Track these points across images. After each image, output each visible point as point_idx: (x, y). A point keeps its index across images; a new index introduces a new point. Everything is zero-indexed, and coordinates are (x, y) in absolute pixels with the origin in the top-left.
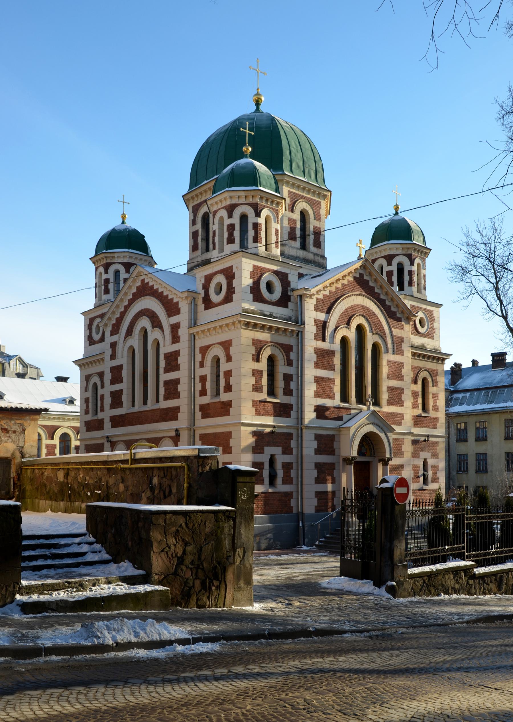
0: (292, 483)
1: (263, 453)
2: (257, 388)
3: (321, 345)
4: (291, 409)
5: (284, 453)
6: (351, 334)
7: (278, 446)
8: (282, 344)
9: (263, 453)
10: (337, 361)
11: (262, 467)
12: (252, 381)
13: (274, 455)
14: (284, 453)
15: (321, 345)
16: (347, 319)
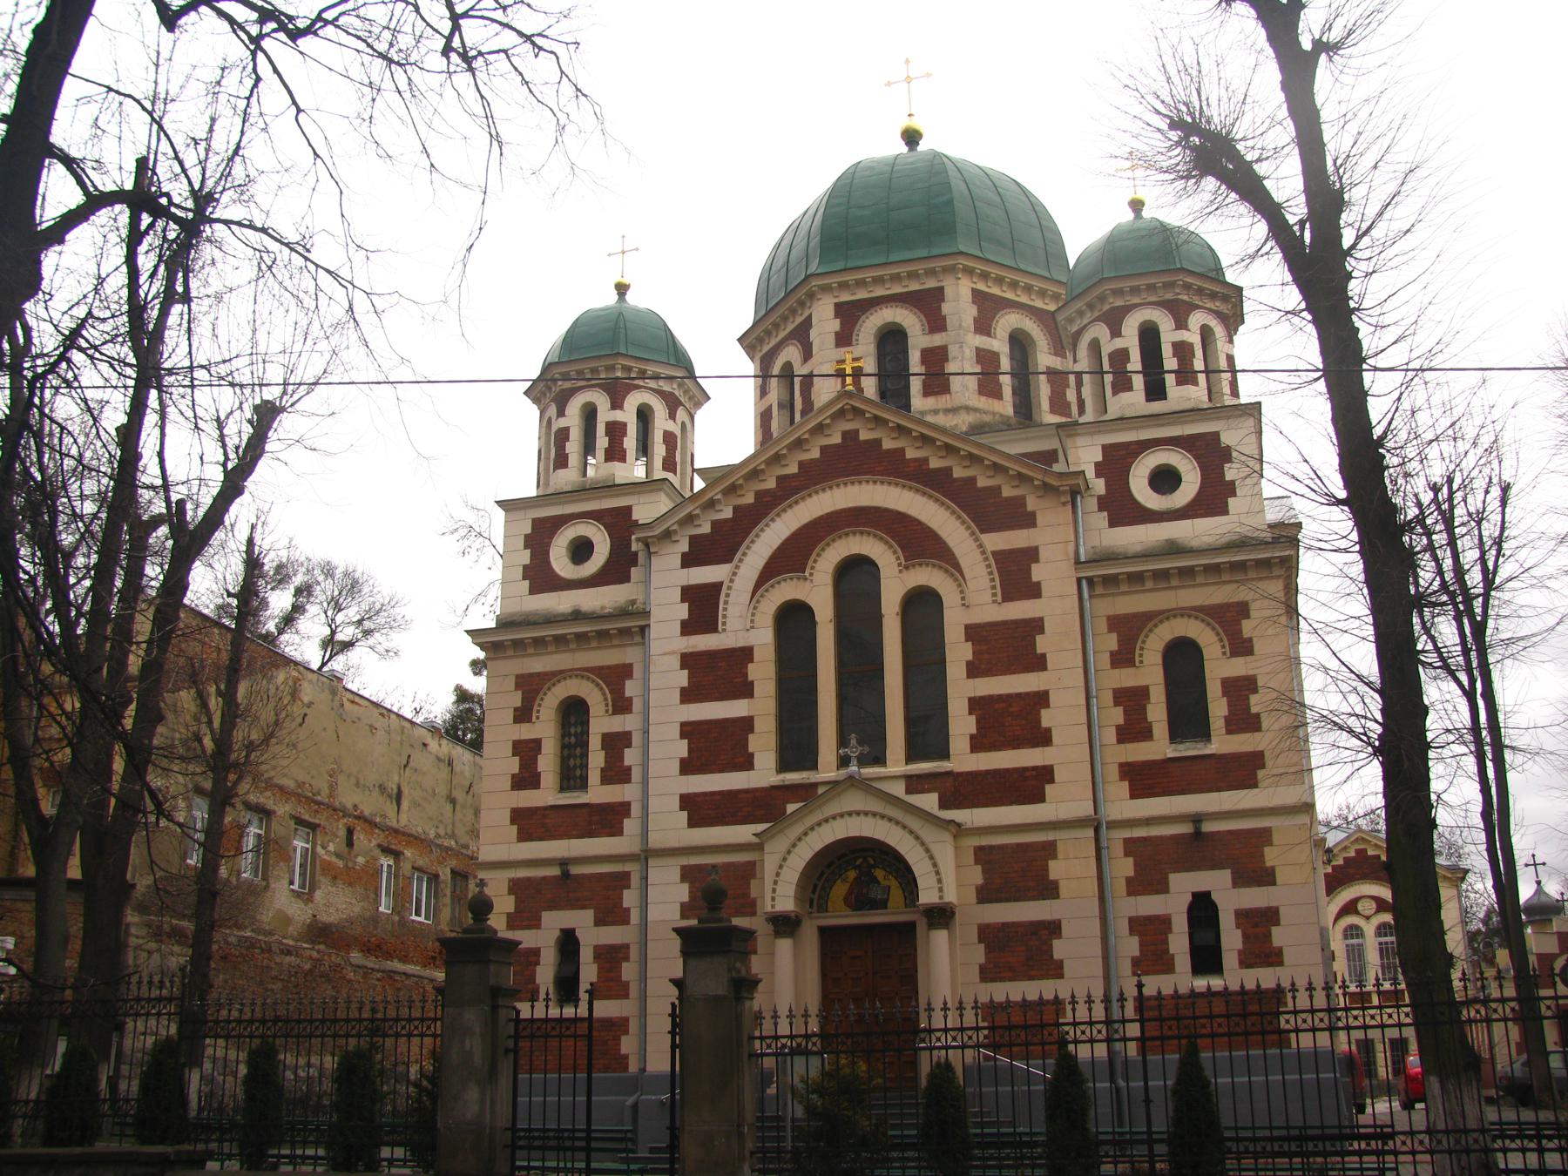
0: (626, 996)
1: (538, 926)
2: (526, 779)
3: (704, 642)
4: (627, 814)
5: (599, 922)
6: (817, 590)
7: (583, 907)
8: (601, 668)
9: (538, 926)
10: (763, 672)
11: (533, 959)
12: (514, 765)
13: (572, 931)
14: (599, 922)
15: (704, 642)
16: (792, 558)
